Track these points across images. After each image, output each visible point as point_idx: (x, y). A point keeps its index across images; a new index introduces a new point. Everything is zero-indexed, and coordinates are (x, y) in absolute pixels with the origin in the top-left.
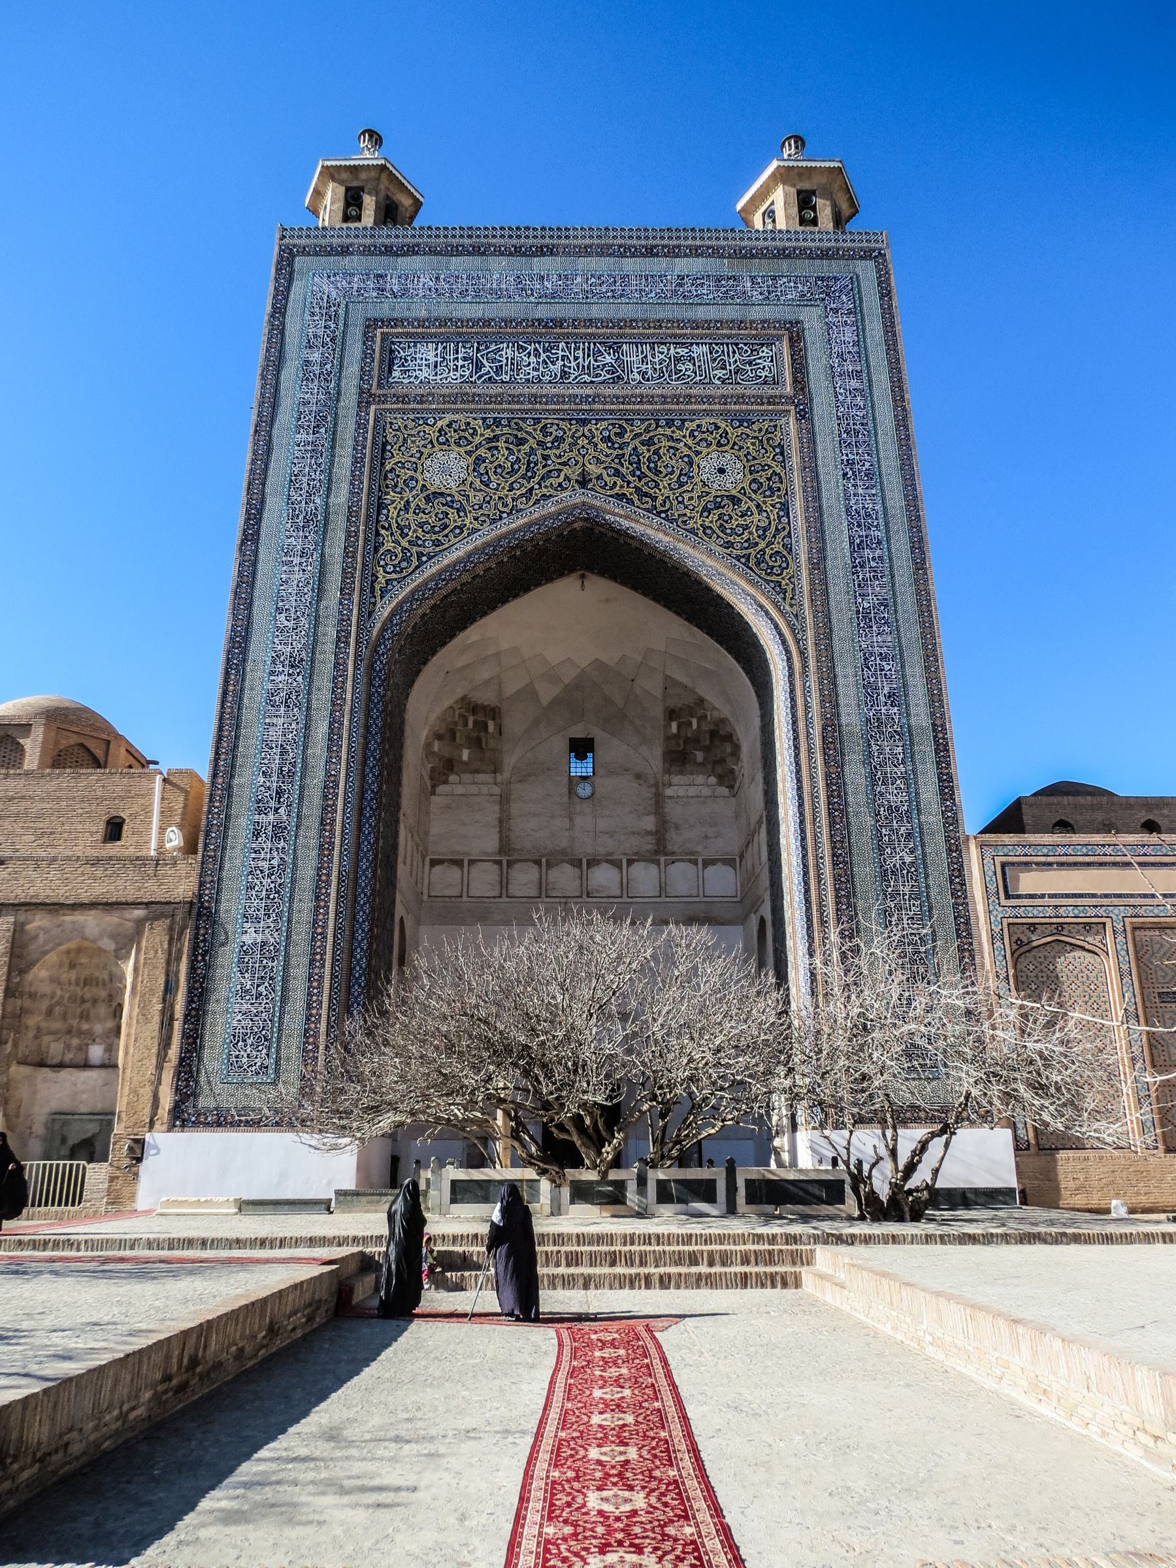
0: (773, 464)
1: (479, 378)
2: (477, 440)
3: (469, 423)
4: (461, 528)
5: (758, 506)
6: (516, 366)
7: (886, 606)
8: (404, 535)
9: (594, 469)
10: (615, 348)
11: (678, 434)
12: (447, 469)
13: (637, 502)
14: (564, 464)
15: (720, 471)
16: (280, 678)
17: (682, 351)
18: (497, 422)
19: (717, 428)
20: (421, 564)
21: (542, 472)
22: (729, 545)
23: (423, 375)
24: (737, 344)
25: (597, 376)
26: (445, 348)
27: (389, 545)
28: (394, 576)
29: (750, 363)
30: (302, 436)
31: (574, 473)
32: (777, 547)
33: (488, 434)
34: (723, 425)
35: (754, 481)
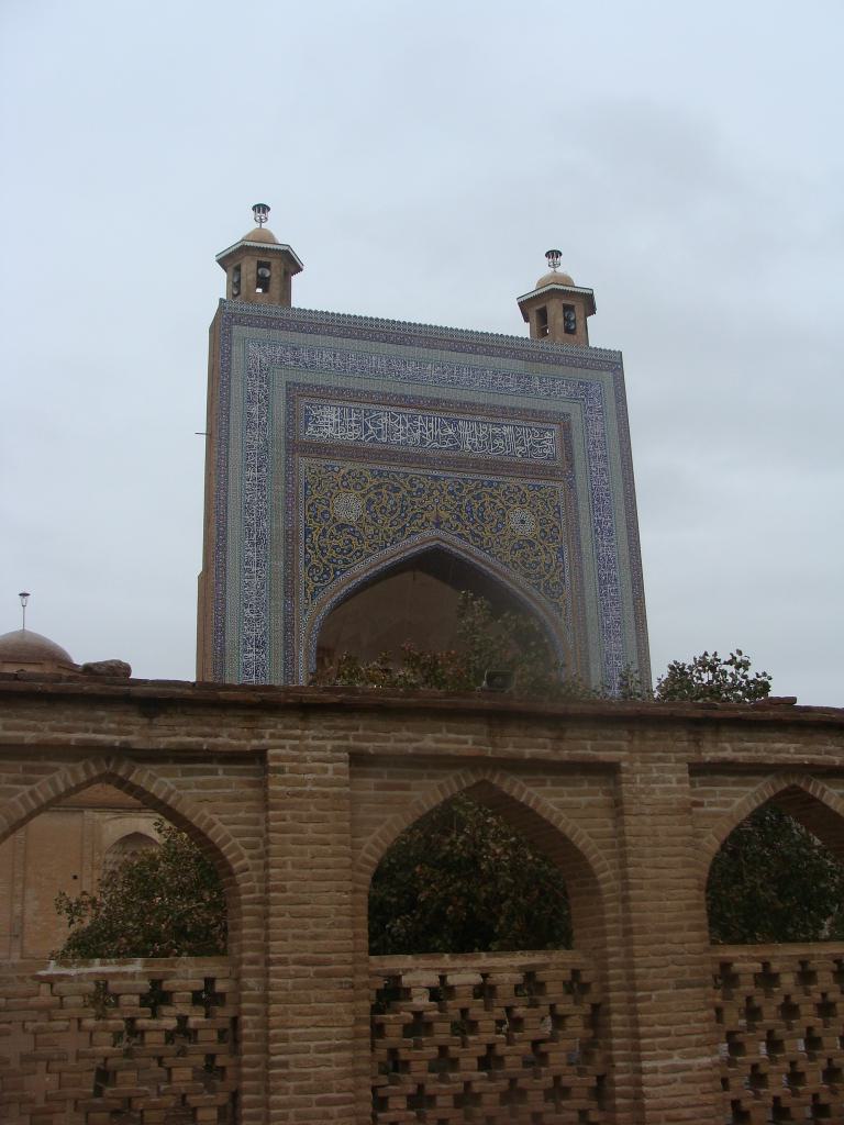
0: (554, 519)
1: (367, 437)
2: (368, 486)
3: (361, 473)
4: (361, 551)
5: (545, 549)
6: (391, 432)
7: (619, 623)
8: (323, 554)
9: (445, 515)
10: (454, 423)
11: (495, 493)
12: (349, 507)
13: (471, 541)
14: (425, 509)
15: (521, 522)
16: (250, 655)
17: (497, 430)
18: (380, 473)
19: (520, 490)
20: (336, 576)
21: (410, 514)
22: (527, 575)
23: (330, 431)
24: (531, 428)
25: (444, 444)
26: (342, 412)
27: (315, 562)
28: (319, 584)
29: (539, 443)
30: (250, 474)
31: (431, 515)
32: (556, 579)
33: (375, 482)
34: (523, 488)
35: (543, 530)
